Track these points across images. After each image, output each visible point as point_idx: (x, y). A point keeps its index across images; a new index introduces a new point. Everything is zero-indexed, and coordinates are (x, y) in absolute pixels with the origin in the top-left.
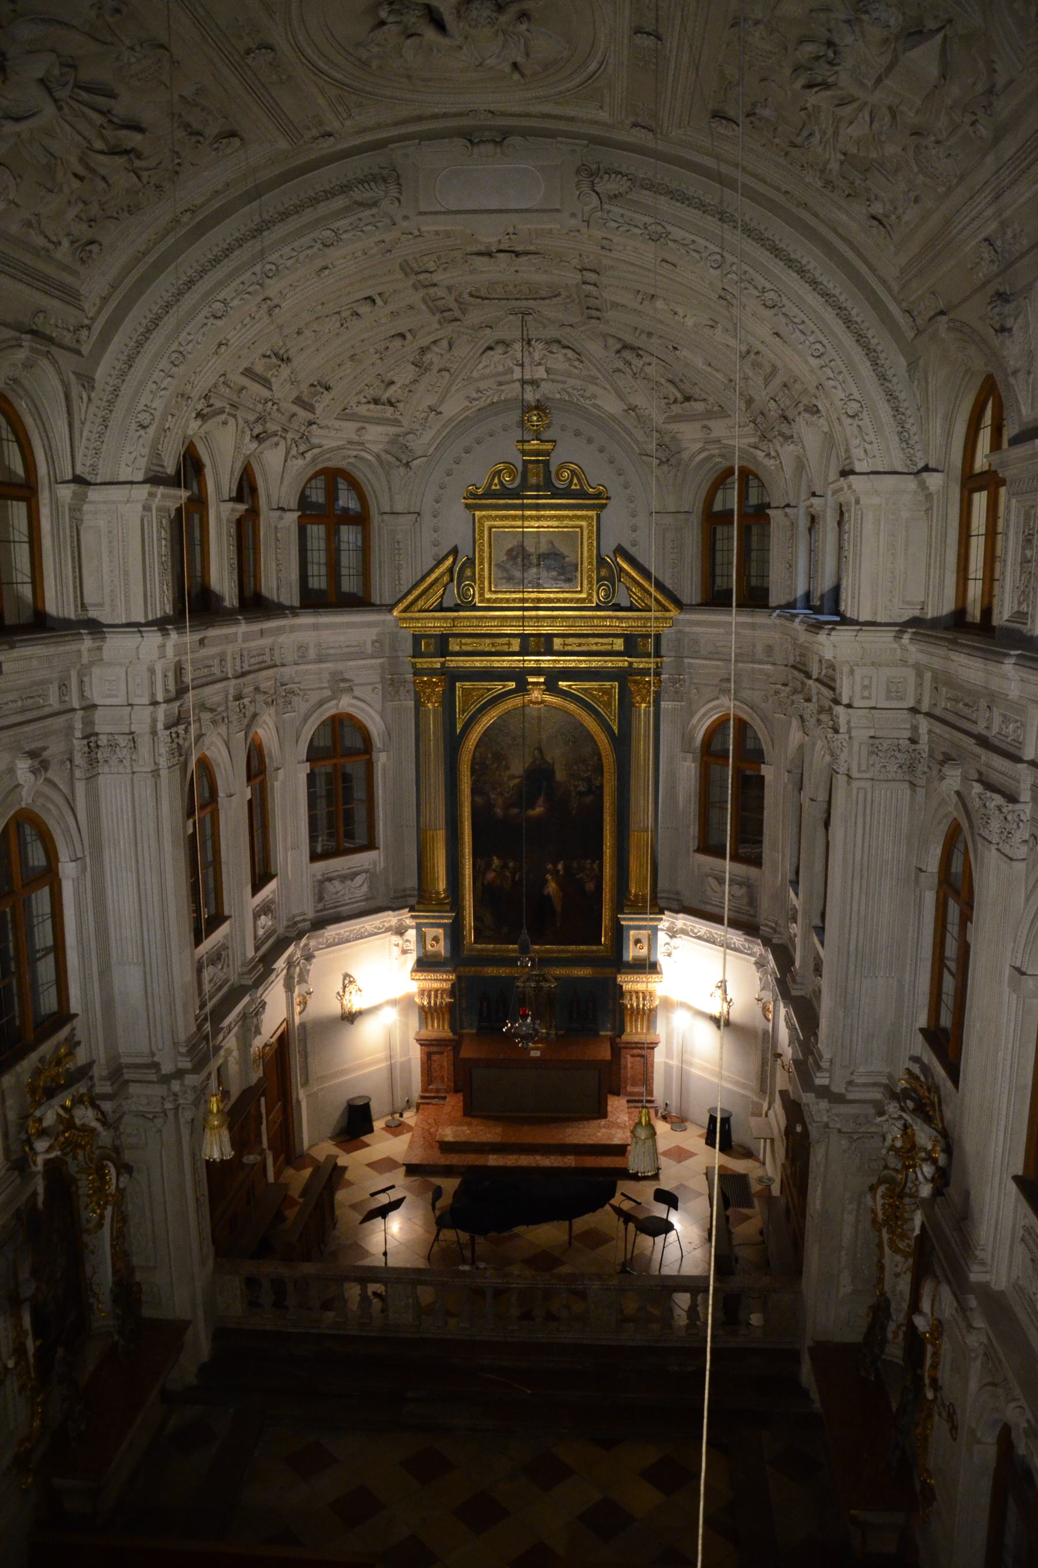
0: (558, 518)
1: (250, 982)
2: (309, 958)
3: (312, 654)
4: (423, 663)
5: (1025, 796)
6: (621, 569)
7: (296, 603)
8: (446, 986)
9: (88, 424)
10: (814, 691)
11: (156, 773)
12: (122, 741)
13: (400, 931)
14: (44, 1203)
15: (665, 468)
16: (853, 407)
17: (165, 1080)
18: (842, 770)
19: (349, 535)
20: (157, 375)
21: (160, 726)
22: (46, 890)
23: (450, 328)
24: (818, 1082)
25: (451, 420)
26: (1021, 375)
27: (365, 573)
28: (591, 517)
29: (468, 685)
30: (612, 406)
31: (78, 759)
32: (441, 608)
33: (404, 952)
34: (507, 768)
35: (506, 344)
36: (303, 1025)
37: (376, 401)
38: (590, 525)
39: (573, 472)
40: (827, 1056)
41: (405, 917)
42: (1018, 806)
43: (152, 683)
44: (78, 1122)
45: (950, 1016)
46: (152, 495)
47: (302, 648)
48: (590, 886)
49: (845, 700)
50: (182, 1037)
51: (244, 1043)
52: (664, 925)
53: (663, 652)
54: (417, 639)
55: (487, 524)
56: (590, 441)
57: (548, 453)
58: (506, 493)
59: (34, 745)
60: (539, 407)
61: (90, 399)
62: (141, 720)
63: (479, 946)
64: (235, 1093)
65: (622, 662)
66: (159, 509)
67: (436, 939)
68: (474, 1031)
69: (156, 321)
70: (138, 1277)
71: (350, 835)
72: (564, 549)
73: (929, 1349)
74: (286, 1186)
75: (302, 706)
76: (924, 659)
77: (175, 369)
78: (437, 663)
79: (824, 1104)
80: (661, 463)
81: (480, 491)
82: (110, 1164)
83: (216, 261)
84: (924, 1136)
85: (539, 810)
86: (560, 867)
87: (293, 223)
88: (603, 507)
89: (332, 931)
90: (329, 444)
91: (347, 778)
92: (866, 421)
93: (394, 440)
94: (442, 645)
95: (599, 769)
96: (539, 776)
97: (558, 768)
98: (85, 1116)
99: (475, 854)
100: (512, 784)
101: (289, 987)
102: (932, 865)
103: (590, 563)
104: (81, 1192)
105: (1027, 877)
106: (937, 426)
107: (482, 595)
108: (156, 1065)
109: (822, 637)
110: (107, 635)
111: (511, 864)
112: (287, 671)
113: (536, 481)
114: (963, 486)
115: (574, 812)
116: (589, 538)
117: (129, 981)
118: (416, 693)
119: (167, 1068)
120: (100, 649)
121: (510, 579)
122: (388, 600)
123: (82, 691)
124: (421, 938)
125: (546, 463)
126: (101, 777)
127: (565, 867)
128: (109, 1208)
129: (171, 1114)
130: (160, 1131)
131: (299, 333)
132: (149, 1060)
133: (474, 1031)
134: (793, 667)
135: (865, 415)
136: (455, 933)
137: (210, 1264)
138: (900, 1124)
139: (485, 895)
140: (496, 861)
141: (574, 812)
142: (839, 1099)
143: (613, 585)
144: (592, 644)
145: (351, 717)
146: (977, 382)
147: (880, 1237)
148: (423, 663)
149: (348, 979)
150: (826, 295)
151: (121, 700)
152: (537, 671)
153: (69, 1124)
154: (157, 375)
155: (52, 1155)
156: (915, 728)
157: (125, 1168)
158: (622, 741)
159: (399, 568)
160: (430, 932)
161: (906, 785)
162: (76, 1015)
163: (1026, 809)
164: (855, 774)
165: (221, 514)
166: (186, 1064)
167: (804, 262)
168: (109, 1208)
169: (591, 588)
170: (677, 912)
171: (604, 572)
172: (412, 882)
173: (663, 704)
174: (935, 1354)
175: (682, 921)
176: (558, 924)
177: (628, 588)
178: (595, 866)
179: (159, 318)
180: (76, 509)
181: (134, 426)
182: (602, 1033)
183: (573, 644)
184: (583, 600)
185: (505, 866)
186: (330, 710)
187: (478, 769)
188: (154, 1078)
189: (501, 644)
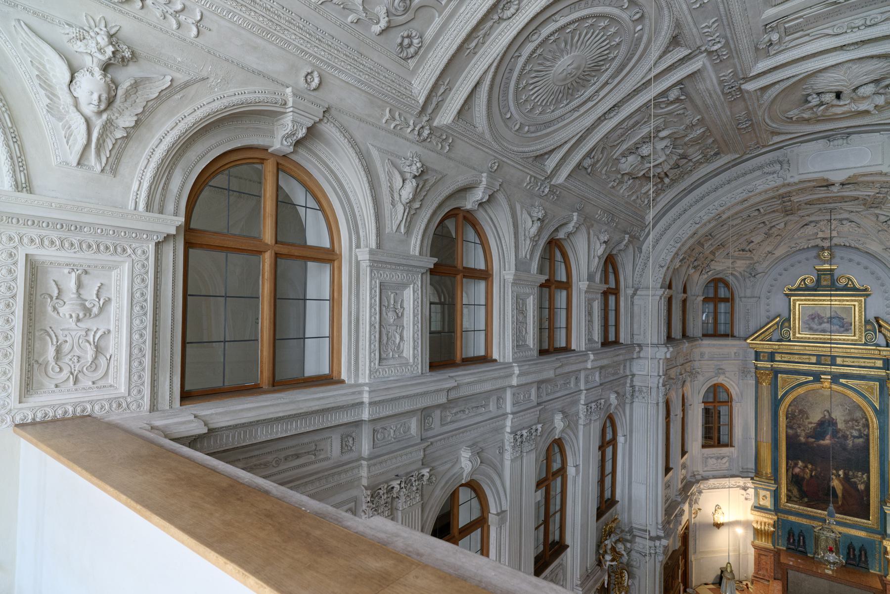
0: (840, 301)
1: (680, 500)
2: (700, 492)
3: (706, 357)
4: (760, 364)
6: (880, 326)
7: (700, 335)
8: (772, 522)
11: (658, 404)
12: (644, 390)
13: (745, 489)
19: (722, 307)
21: (660, 385)
22: (611, 447)
23: (787, 218)
25: (777, 258)
28: (861, 301)
29: (785, 376)
30: (874, 247)
32: (770, 340)
33: (746, 499)
34: (807, 418)
35: (817, 222)
36: (695, 524)
37: (743, 250)
39: (849, 279)
41: (749, 483)
47: (702, 355)
48: (861, 487)
50: (660, 521)
51: (676, 528)
54: (757, 354)
55: (798, 303)
56: (858, 264)
57: (831, 270)
58: (807, 289)
60: (830, 248)
62: (653, 382)
65: (882, 373)
69: (669, 227)
72: (844, 316)
75: (701, 378)
78: (768, 365)
81: (794, 288)
83: (697, 201)
85: (827, 441)
86: (841, 473)
87: (734, 184)
88: (868, 295)
89: (712, 482)
90: (719, 268)
93: (748, 267)
94: (771, 357)
95: (867, 426)
98: (620, 547)
99: (788, 458)
100: (810, 426)
101: (691, 506)
103: (860, 322)
112: (696, 364)
113: (825, 283)
117: (640, 492)
119: (653, 534)
120: (639, 352)
121: (811, 329)
122: (742, 334)
124: (757, 495)
125: (832, 275)
126: (634, 404)
127: (845, 474)
129: (653, 556)
136: (776, 495)
139: (795, 481)
140: (800, 464)
143: (876, 334)
144: (862, 362)
148: (760, 364)
149: (718, 507)
152: (829, 373)
153: (613, 549)
157: (631, 576)
159: (748, 321)
160: (762, 493)
165: (678, 298)
169: (861, 335)
171: (868, 327)
172: (751, 465)
177: (884, 335)
178: (864, 476)
180: (632, 297)
183: (849, 361)
184: (856, 340)
186: (715, 381)
189: (805, 358)
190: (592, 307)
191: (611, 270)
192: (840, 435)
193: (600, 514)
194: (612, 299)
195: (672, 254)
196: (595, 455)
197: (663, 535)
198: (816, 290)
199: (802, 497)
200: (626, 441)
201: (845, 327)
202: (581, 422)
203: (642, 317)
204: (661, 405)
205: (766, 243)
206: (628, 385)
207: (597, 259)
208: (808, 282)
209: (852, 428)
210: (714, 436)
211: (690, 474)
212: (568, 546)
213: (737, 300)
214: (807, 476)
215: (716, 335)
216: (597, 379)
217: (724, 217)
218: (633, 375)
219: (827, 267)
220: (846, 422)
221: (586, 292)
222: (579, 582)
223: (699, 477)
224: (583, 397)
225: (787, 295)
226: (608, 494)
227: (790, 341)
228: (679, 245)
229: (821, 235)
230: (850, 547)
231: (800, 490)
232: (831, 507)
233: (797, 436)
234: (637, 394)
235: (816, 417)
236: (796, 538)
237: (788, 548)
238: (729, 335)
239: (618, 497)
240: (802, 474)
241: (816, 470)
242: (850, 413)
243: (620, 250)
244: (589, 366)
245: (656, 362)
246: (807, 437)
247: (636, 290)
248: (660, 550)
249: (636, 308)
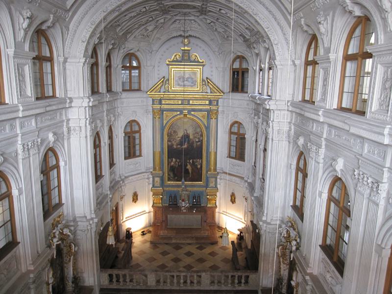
0: (192, 68)
5: (323, 147)
6: (208, 82)
7: (121, 90)
9: (67, 40)
10: (261, 116)
13: (148, 178)
14: (56, 256)
15: (221, 55)
16: (276, 42)
17: (88, 221)
18: (271, 138)
20: (87, 27)
21: (88, 124)
22: (56, 170)
24: (263, 219)
26: (325, 36)
27: (140, 83)
30: (206, 38)
31: (65, 133)
34: (177, 135)
35: (180, 20)
37: (143, 35)
38: (200, 70)
39: (196, 56)
40: (265, 212)
42: (321, 149)
43: (86, 113)
44: (65, 233)
45: (299, 203)
46: (86, 61)
47: (122, 103)
48: (199, 166)
49: (272, 120)
50: (93, 209)
52: (219, 177)
53: (219, 105)
54: (153, 100)
55: (173, 69)
57: (189, 50)
59: (54, 130)
61: (68, 33)
63: (169, 182)
64: (104, 224)
66: (87, 64)
67: (157, 182)
68: (167, 205)
70: (79, 275)
71: (134, 153)
72: (193, 77)
73: (295, 290)
74: (118, 248)
76: (294, 109)
77: (92, 26)
78: (158, 107)
79: (265, 225)
80: (219, 54)
81: (171, 60)
82: (73, 244)
84: (293, 234)
86: (191, 161)
88: (203, 66)
91: (134, 139)
92: (279, 46)
95: (202, 135)
96: (186, 137)
97: (190, 135)
98: (66, 231)
99: (168, 158)
102: (295, 163)
103: (200, 80)
104: (64, 252)
105: (324, 168)
106: (299, 48)
107: (171, 88)
108: (86, 217)
109: (266, 103)
110: (74, 100)
111: (178, 160)
113: (186, 58)
114: (305, 64)
115: (195, 147)
116: (200, 74)
118: (154, 114)
123: (66, 115)
124: (153, 181)
125: (189, 53)
126: (71, 139)
127: (193, 162)
128: (72, 257)
129: (90, 230)
130: (86, 235)
131: (125, 16)
132: (83, 215)
133: (167, 205)
134: (254, 110)
135: (279, 45)
137: (99, 270)
138: (286, 230)
139: (172, 169)
140: (174, 160)
141: (195, 147)
142: (269, 224)
145: (134, 121)
146: (310, 37)
147: (280, 260)
150: (270, 12)
151: (77, 117)
153: (61, 233)
154: (87, 27)
155: (58, 243)
156: (290, 128)
158: (208, 128)
159: (149, 81)
161: (288, 142)
162: (64, 204)
163: (322, 151)
164: (274, 139)
166: (93, 216)
167: (264, 2)
168: (72, 257)
170: (222, 173)
173: (219, 118)
175: (223, 176)
176: (190, 176)
179: (88, 11)
181: (81, 41)
182: (202, 205)
185: (176, 161)
187: (169, 135)
188: (85, 220)
190: (23, 70)
191: (43, 40)
192: (191, 142)
193: (46, 214)
194: (47, 66)
195: (90, 33)
196: (36, 176)
197: (95, 216)
198: (181, 62)
199: (174, 177)
200: (66, 165)
201: (194, 83)
202: (20, 157)
203: (72, 78)
204: (89, 137)
205: (155, 32)
206: (65, 126)
207: (22, 32)
208: (178, 57)
209: (196, 137)
210: (132, 151)
211: (118, 176)
212: (19, 243)
213: (142, 68)
214: (177, 166)
215: (131, 90)
216: (34, 124)
217: (123, 9)
218: (68, 120)
219: (186, 48)
220: (194, 134)
221: (14, 58)
222: (31, 262)
223: (123, 177)
224: (19, 138)
225: (168, 65)
226: (55, 201)
227: (169, 92)
228: (93, 27)
229: (182, 29)
230: (194, 197)
231: (174, 173)
232: (183, 180)
233: (172, 145)
234: (72, 132)
235: (181, 134)
236: (173, 198)
237: (169, 204)
238: (139, 90)
239: (64, 201)
240: (174, 165)
241: (180, 162)
242: (195, 130)
243: (49, 27)
244: (21, 116)
245: (83, 109)
246: (177, 145)
247: (67, 58)
248: (94, 226)
249: (68, 72)
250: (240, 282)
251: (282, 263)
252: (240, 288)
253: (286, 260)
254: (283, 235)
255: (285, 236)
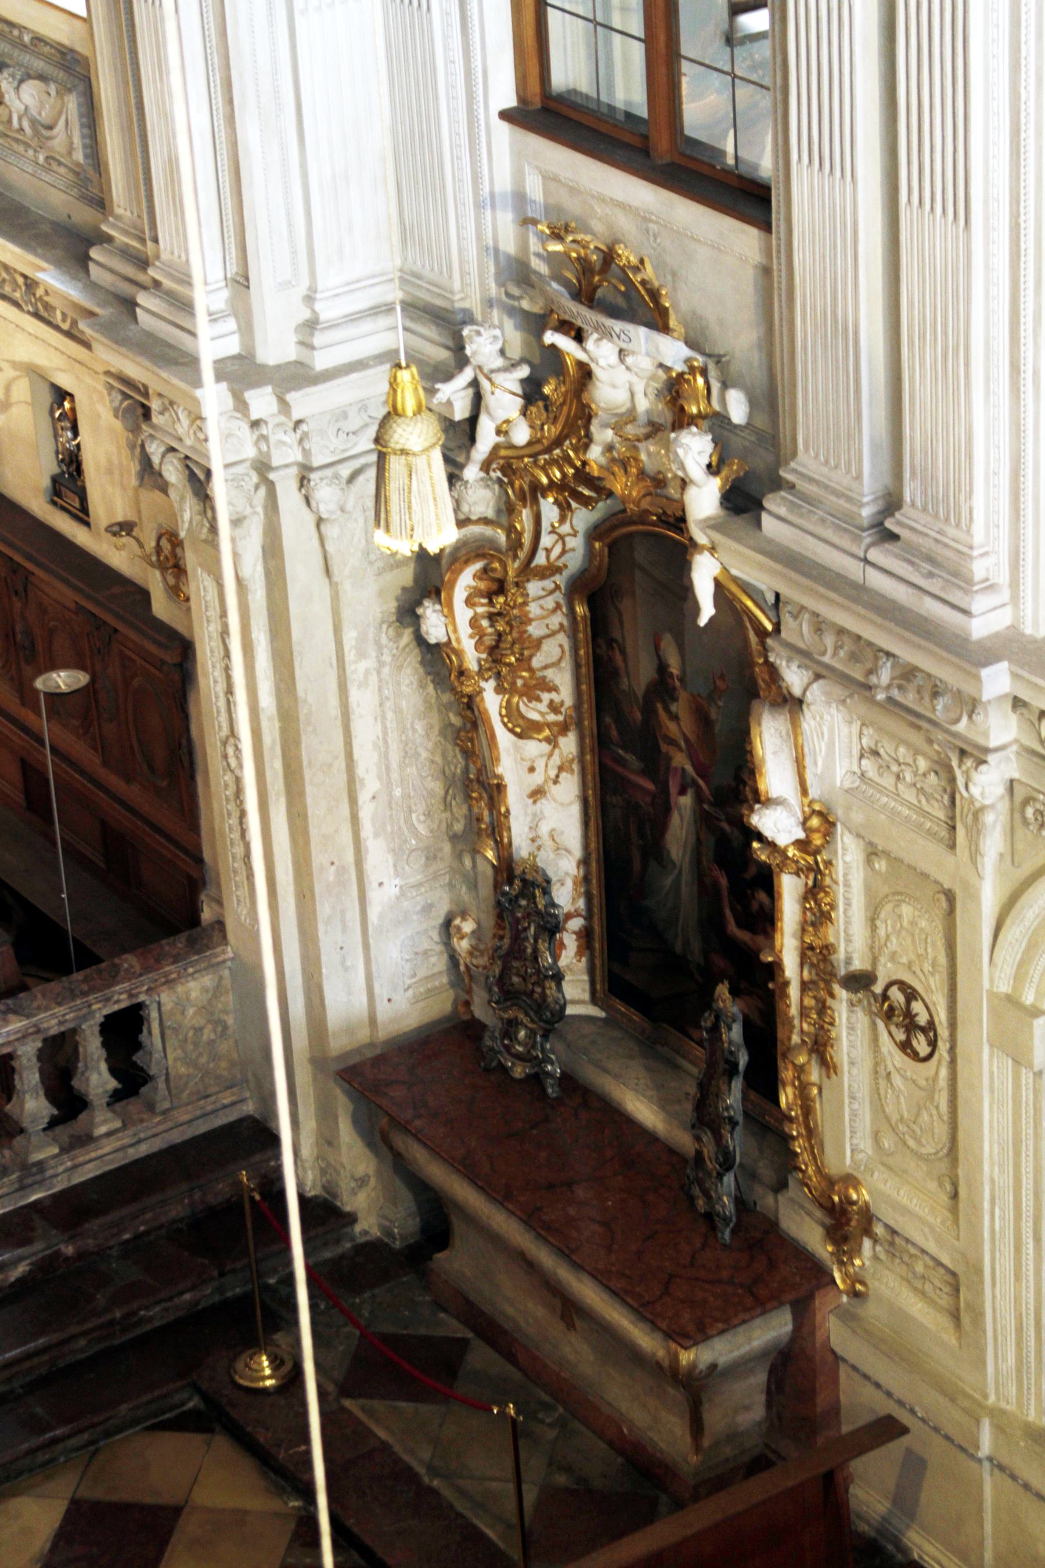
73: (790, 888)
142: (296, 376)
174: (814, 892)
250: (69, 1104)
251: (504, 738)
252: (89, 1166)
253: (539, 686)
254: (486, 438)
255: (521, 435)
